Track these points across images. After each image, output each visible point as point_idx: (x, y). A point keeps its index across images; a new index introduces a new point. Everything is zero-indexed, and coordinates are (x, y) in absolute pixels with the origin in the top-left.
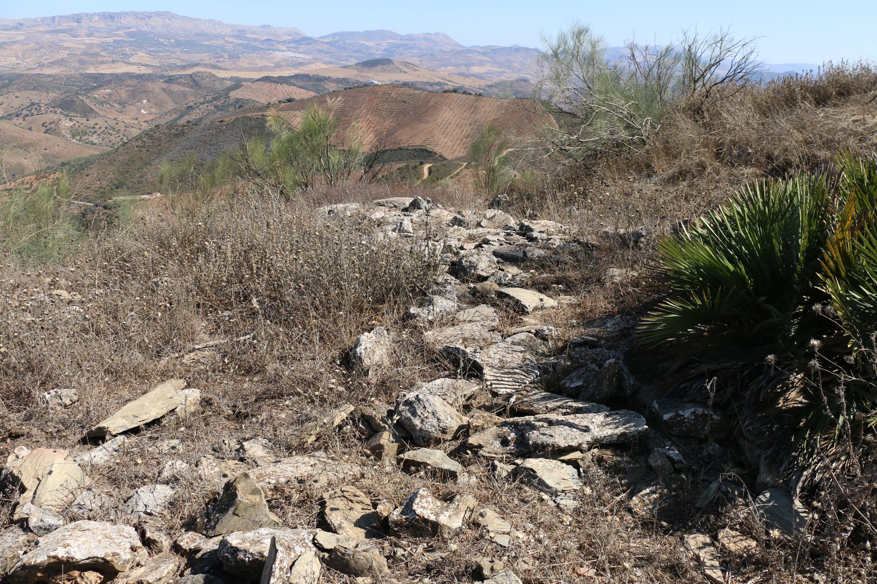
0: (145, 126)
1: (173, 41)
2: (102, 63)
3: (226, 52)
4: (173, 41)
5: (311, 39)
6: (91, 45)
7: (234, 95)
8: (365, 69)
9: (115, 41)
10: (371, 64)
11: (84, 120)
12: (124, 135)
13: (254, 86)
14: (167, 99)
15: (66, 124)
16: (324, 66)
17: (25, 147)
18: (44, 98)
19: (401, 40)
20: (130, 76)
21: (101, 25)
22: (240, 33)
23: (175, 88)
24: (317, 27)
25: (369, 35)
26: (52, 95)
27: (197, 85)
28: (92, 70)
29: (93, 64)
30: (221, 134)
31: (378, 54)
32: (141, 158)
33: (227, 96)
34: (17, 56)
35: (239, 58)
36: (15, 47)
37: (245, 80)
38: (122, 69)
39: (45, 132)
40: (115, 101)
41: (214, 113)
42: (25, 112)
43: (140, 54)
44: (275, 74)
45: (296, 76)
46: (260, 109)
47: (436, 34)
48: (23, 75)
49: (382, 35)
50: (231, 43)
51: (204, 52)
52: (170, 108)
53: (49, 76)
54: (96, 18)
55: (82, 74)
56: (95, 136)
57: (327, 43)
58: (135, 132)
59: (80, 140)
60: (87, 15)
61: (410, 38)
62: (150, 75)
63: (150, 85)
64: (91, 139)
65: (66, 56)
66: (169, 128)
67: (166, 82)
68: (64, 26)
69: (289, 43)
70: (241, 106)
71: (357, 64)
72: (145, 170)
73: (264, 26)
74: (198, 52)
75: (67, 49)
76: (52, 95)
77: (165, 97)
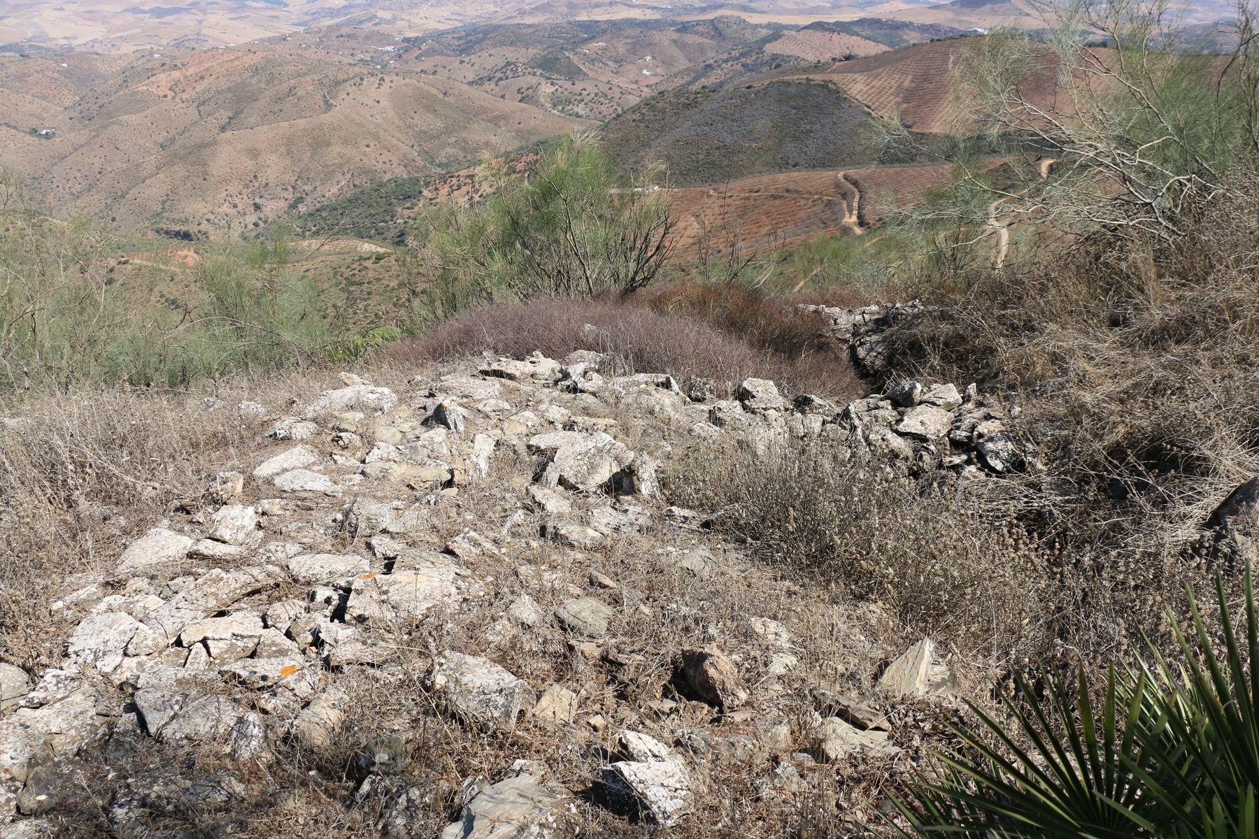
0: (647, 92)
7: (771, 49)
11: (568, 85)
15: (547, 89)
16: (904, 6)
17: (496, 120)
18: (521, 55)
20: (631, 23)
23: (690, 39)
26: (532, 51)
28: (583, 17)
29: (585, 8)
30: (748, 106)
32: (638, 137)
33: (760, 50)
37: (787, 27)
38: (621, 14)
40: (610, 58)
41: (741, 74)
42: (499, 75)
44: (831, 19)
45: (862, 22)
46: (805, 70)
48: (499, 26)
52: (682, 67)
53: (530, 26)
55: (570, 23)
56: (582, 105)
58: (633, 100)
59: (562, 111)
62: (657, 21)
64: (576, 109)
67: (678, 31)
70: (778, 66)
72: (642, 153)
76: (532, 51)
77: (675, 51)
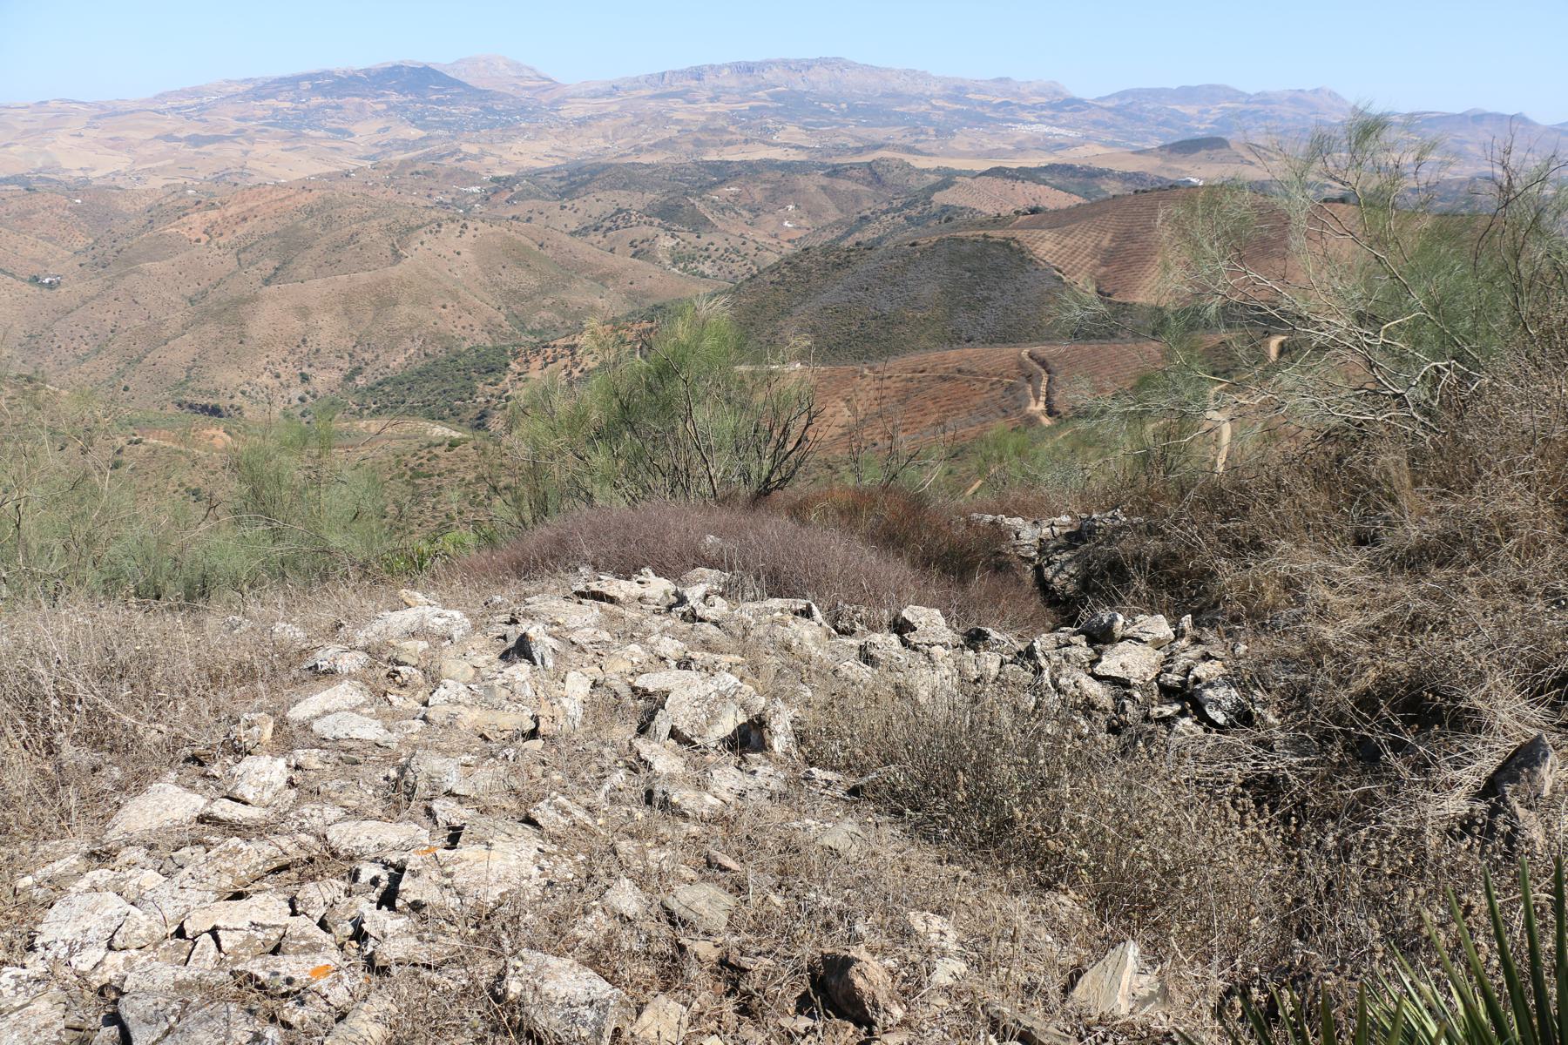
0: (789, 249)
1: (844, 106)
2: (729, 143)
3: (931, 123)
4: (844, 106)
5: (1081, 101)
6: (715, 115)
7: (940, 198)
8: (1175, 156)
9: (752, 108)
10: (1188, 147)
11: (692, 238)
12: (753, 263)
13: (976, 184)
14: (830, 205)
15: (666, 242)
16: (1101, 151)
17: (603, 279)
18: (635, 201)
19: (1247, 102)
20: (770, 164)
21: (733, 82)
22: (958, 92)
23: (843, 185)
24: (1095, 74)
25: (1187, 94)
26: (649, 196)
27: (879, 180)
28: (712, 156)
29: (714, 146)
30: (911, 267)
31: (1201, 130)
32: (776, 303)
33: (928, 200)
34: (605, 137)
35: (953, 134)
36: (606, 122)
37: (960, 173)
38: (759, 153)
39: (633, 256)
40: (743, 207)
41: (904, 229)
42: (607, 224)
43: (791, 128)
44: (1014, 164)
45: (1051, 168)
46: (982, 225)
47: (1316, 91)
48: (610, 166)
49: (1211, 93)
50: (942, 108)
51: (895, 125)
52: (832, 219)
53: (647, 166)
54: (726, 72)
55: (696, 163)
56: (708, 263)
57: (1109, 109)
58: (771, 258)
59: (684, 269)
60: (712, 67)
61: (1264, 99)
62: (802, 162)
63: (802, 181)
64: (701, 268)
65: (675, 133)
66: (825, 254)
67: (828, 175)
68: (677, 86)
69: (1043, 108)
70: (949, 219)
71: (1161, 148)
72: (781, 323)
73: (1000, 80)
74: (885, 125)
75: (678, 122)
76: (649, 196)
77: (823, 200)
